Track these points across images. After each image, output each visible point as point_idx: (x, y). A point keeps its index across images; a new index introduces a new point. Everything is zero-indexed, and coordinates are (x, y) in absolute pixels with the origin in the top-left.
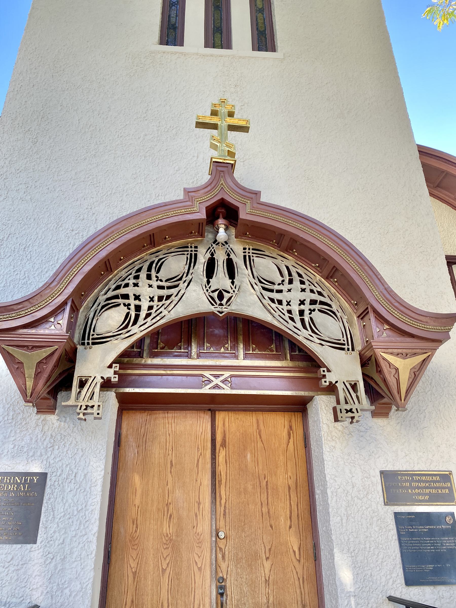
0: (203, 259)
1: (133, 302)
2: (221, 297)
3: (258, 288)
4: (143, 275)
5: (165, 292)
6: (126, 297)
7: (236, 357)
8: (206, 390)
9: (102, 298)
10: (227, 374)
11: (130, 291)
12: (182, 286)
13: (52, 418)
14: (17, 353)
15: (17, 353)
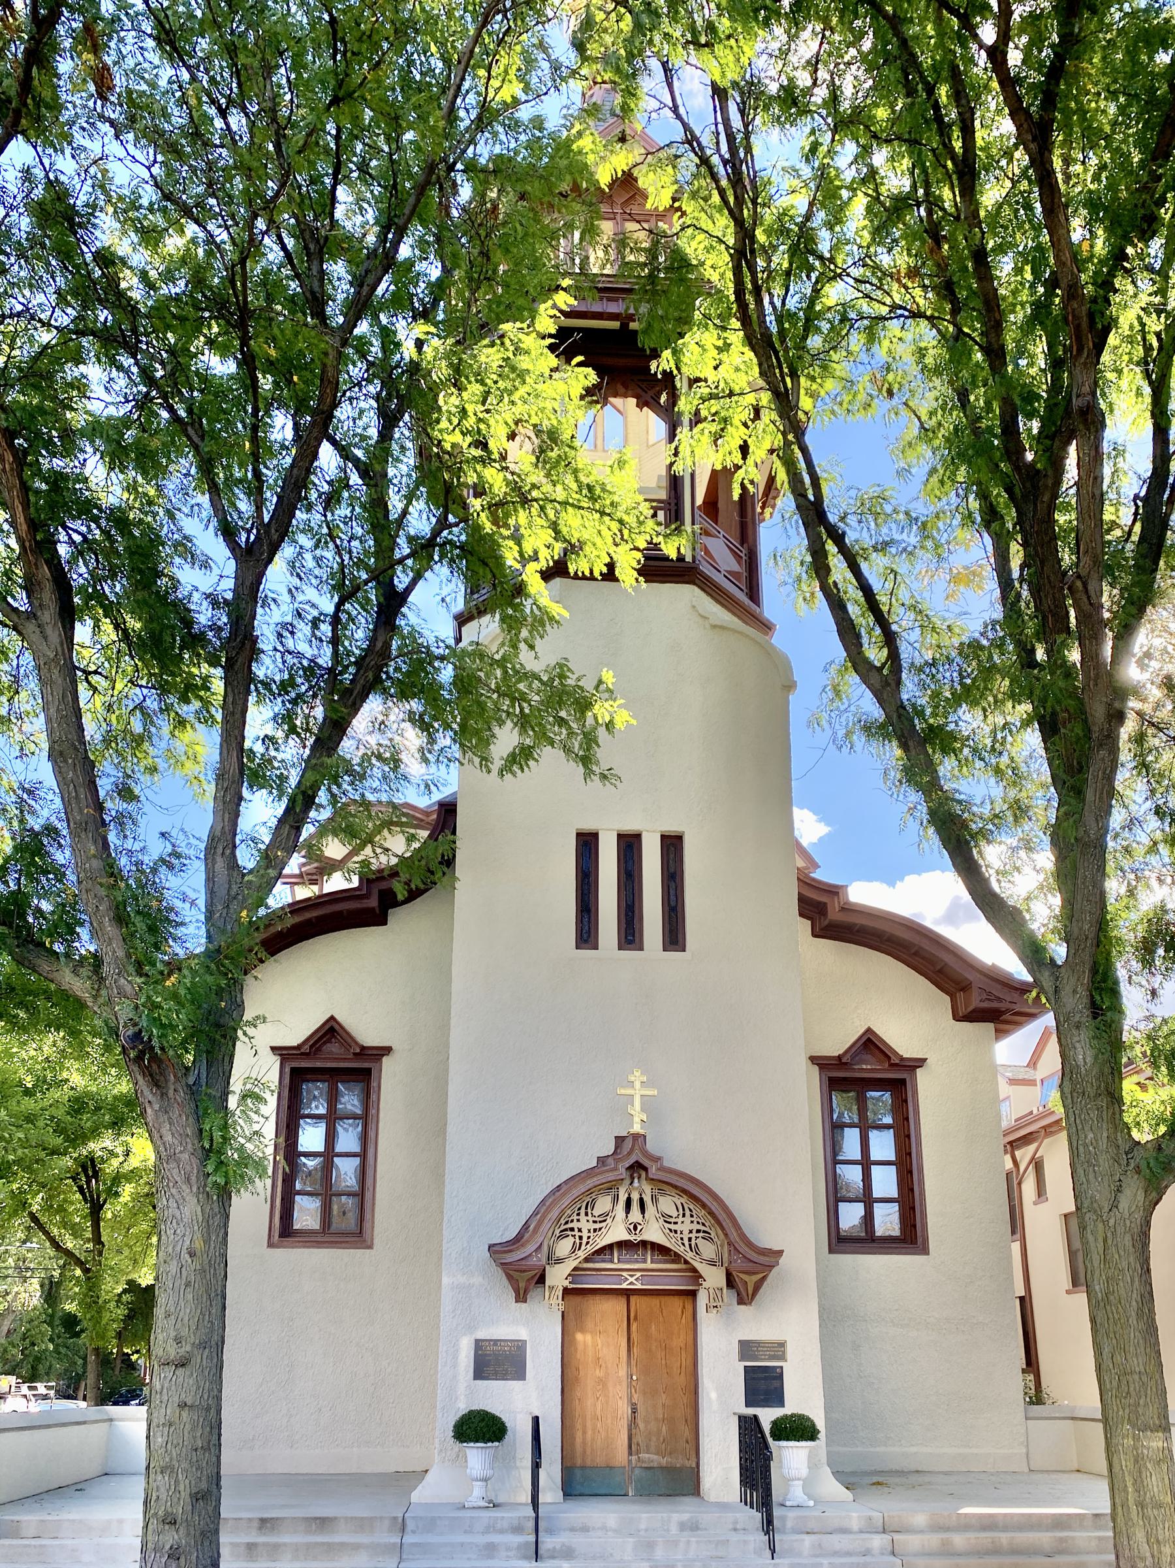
0: (623, 1198)
1: (576, 1233)
2: (635, 1228)
3: (661, 1221)
4: (583, 1211)
5: (597, 1226)
6: (572, 1229)
7: (645, 1261)
8: (624, 1286)
9: (557, 1232)
10: (639, 1274)
11: (575, 1225)
12: (609, 1220)
13: (524, 1305)
14: (515, 1275)
15: (515, 1275)
